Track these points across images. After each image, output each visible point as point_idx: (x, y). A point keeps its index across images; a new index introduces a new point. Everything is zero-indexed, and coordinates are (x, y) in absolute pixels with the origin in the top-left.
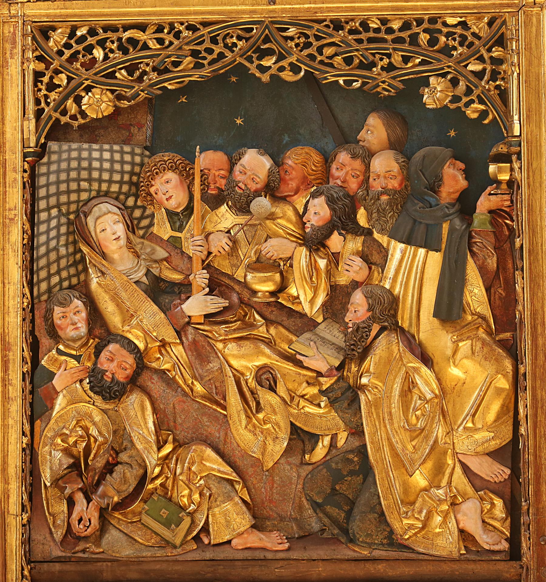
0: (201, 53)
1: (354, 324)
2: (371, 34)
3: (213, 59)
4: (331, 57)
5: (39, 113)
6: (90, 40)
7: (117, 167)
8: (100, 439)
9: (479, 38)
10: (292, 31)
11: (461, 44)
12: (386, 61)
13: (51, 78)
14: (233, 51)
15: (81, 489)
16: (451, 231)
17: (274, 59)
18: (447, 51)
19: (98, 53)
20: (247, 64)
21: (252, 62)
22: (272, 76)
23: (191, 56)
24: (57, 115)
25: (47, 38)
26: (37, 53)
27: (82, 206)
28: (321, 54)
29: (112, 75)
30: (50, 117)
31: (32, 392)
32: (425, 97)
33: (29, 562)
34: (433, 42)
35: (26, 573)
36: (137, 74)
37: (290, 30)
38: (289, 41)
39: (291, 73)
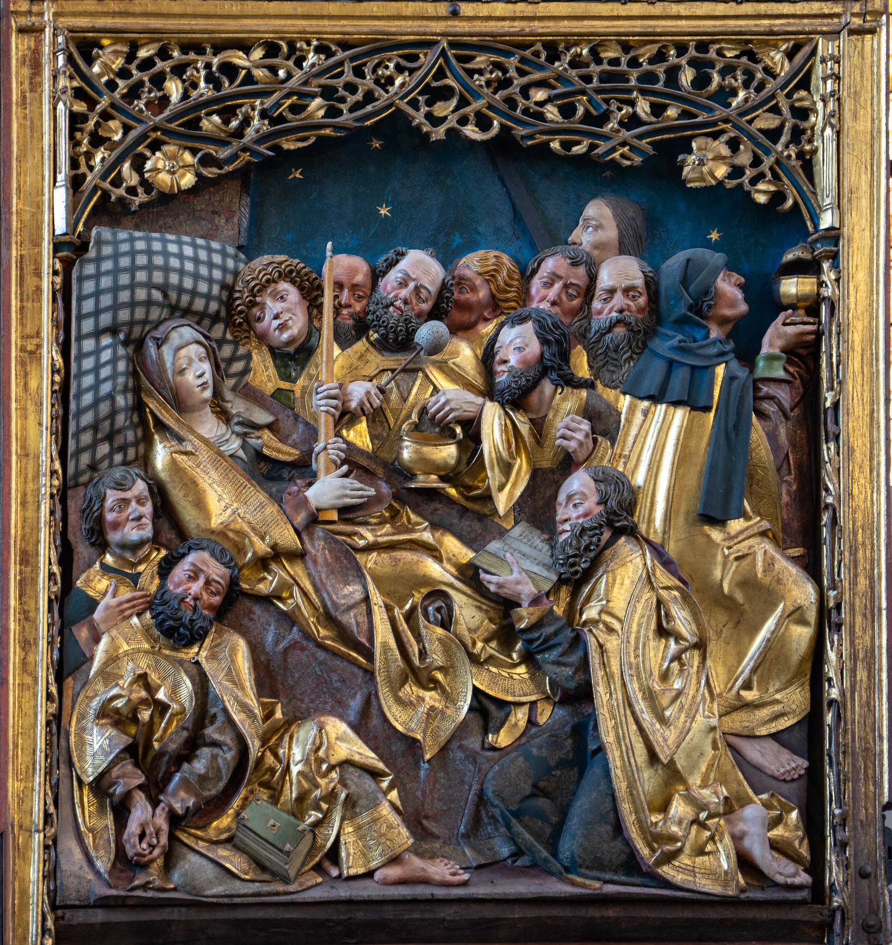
0: (337, 91)
1: (574, 527)
2: (606, 67)
3: (358, 102)
4: (541, 104)
5: (76, 183)
6: (160, 65)
7: (204, 271)
8: (175, 706)
9: (774, 76)
10: (481, 60)
11: (746, 85)
12: (626, 110)
13: (98, 124)
14: (387, 92)
15: (140, 787)
16: (730, 379)
17: (454, 102)
18: (725, 95)
19: (174, 88)
20: (410, 111)
21: (417, 109)
22: (450, 132)
23: (321, 96)
24: (106, 185)
25: (90, 62)
26: (75, 84)
27: (149, 332)
28: (527, 97)
29: (194, 124)
30: (96, 188)
31: (61, 633)
32: (686, 170)
33: (54, 907)
34: (701, 81)
35: (50, 924)
36: (234, 124)
37: (478, 59)
38: (476, 76)
39: (477, 129)
